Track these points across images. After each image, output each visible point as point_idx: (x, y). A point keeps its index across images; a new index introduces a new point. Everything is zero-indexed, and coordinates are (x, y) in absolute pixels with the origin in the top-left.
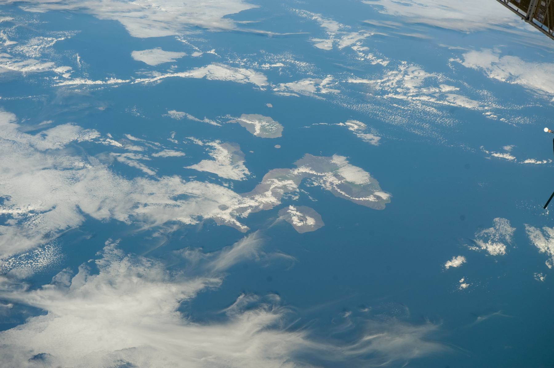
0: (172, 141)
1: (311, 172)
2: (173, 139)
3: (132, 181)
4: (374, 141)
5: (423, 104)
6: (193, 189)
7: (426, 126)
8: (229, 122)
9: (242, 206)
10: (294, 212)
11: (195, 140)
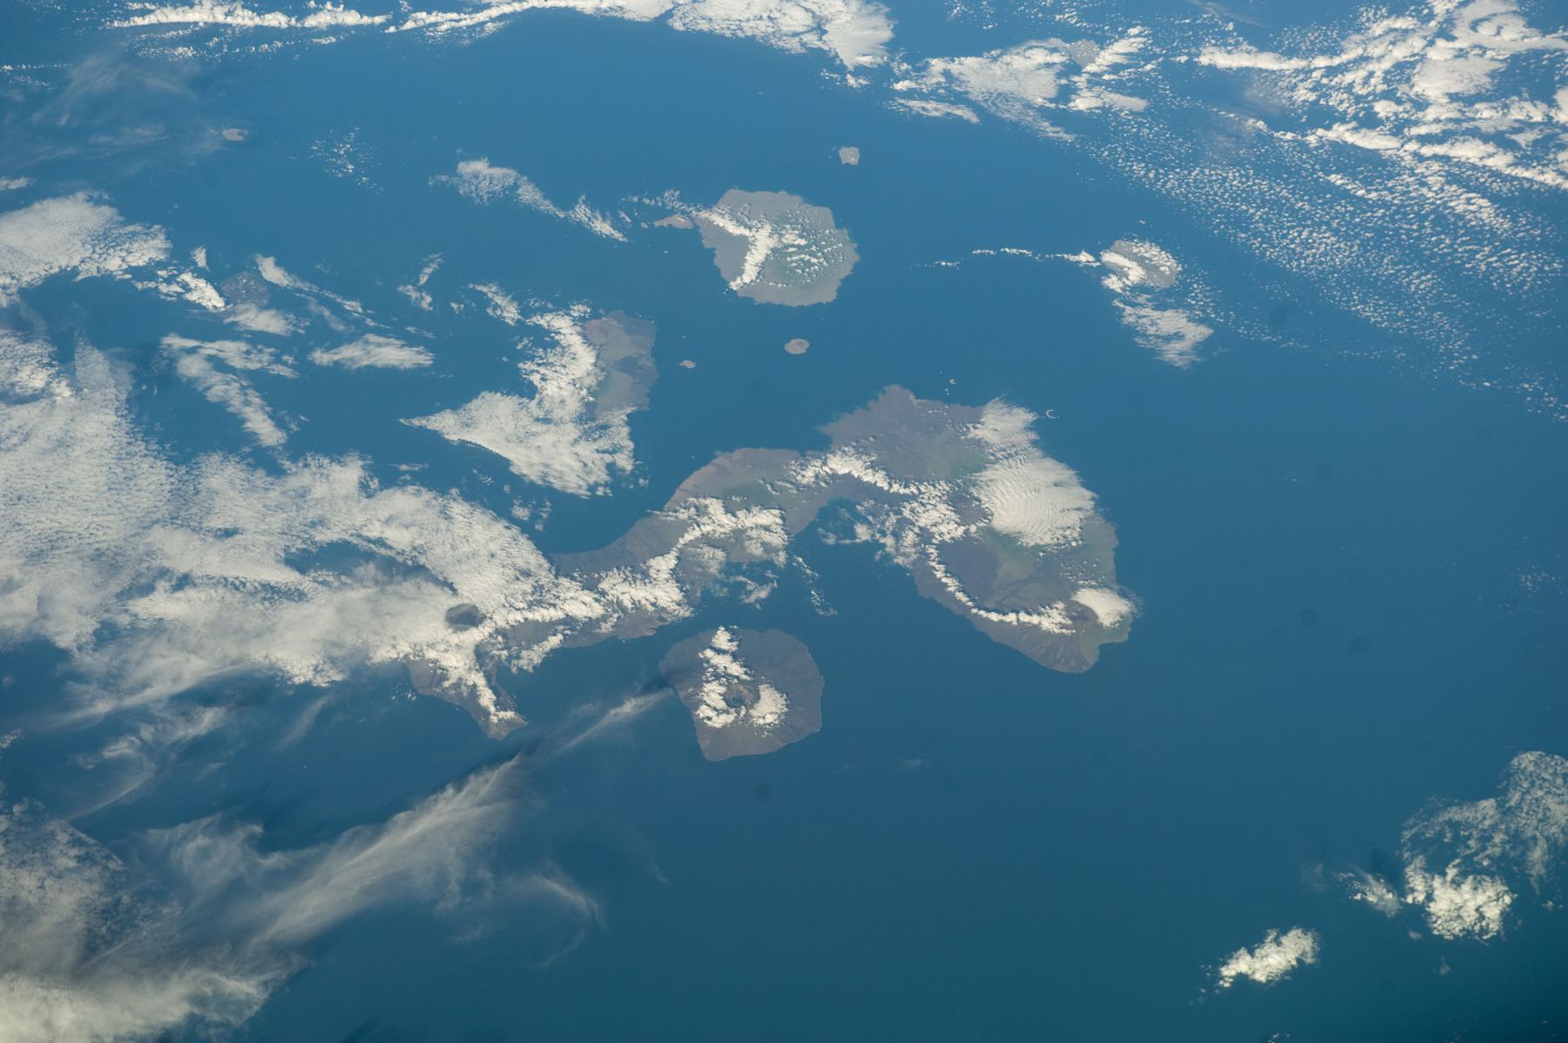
0: (414, 295)
1: (868, 477)
2: (419, 289)
3: (183, 470)
4: (1178, 346)
5: (1452, 179)
6: (388, 521)
7: (1421, 282)
8: (665, 223)
9: (539, 615)
10: (722, 662)
11: (499, 300)
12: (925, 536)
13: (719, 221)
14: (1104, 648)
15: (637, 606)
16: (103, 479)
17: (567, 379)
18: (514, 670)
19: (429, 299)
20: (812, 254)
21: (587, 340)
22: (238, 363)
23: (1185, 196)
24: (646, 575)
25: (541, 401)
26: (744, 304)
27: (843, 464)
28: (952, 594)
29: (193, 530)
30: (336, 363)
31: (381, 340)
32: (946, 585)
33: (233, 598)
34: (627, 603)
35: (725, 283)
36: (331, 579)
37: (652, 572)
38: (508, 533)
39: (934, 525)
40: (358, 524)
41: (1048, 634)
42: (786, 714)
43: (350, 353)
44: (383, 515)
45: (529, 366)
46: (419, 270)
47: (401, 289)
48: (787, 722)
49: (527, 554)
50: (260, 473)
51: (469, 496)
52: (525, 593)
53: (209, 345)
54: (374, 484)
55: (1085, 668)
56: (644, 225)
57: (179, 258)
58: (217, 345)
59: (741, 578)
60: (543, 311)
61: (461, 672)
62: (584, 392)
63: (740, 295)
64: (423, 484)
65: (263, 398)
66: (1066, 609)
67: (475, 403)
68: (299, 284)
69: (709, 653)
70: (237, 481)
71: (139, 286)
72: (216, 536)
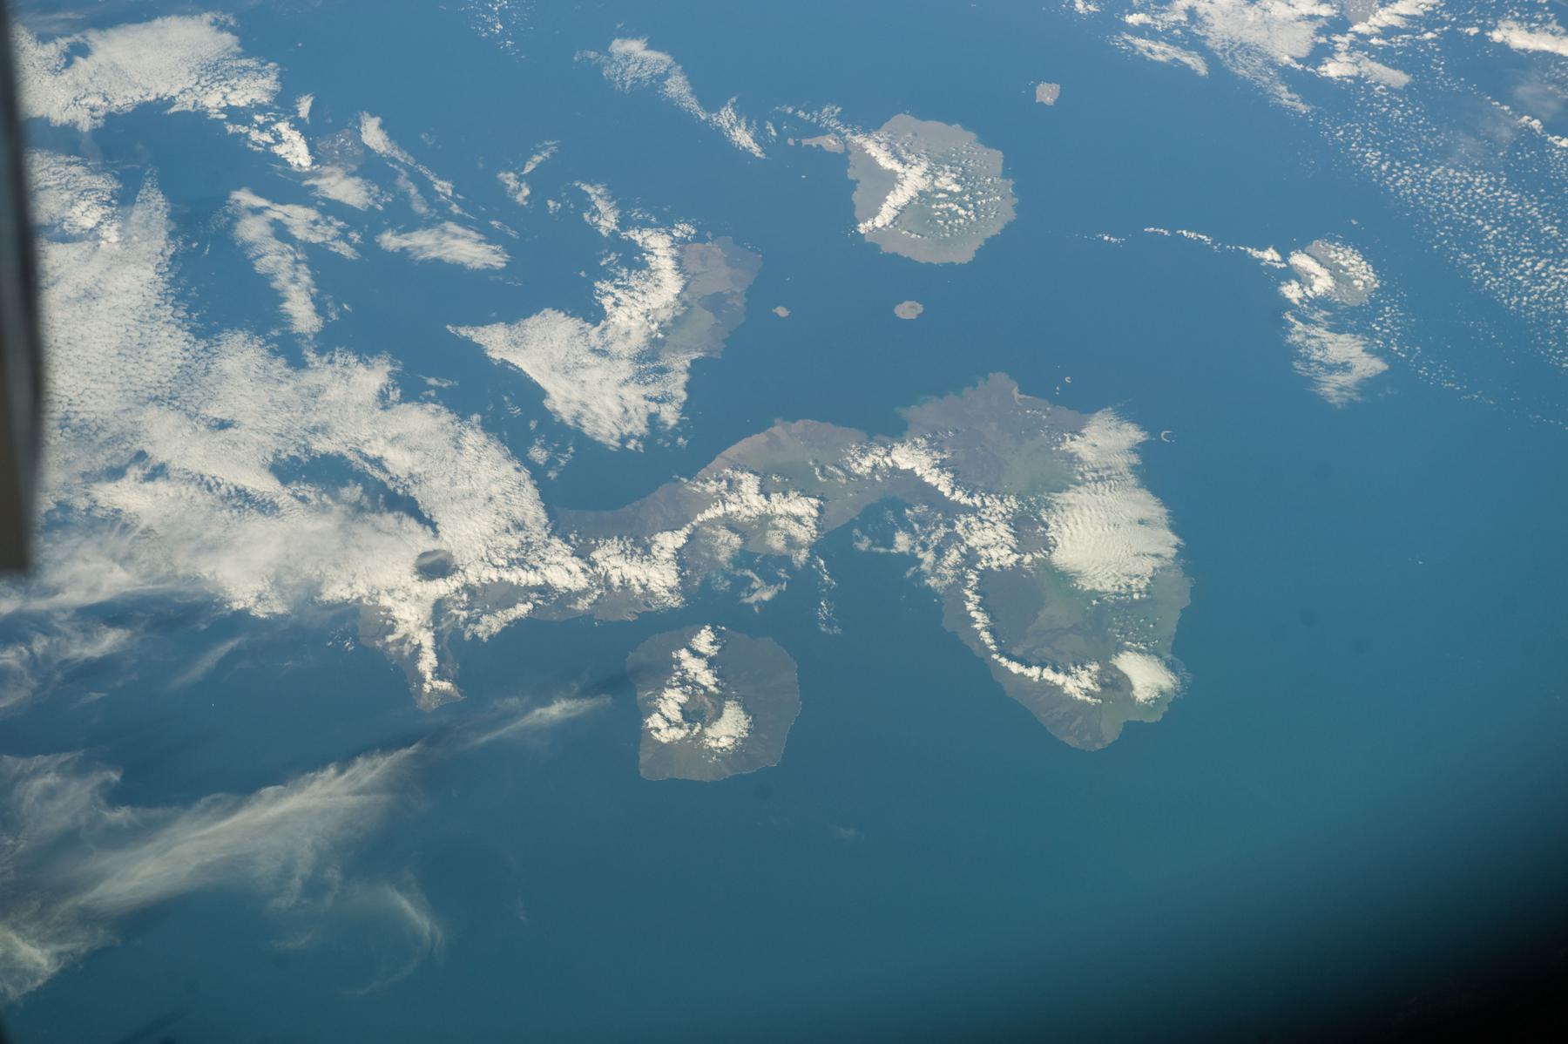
0: (513, 184)
1: (932, 478)
2: (520, 179)
3: (202, 344)
4: (1341, 379)
6: (393, 441)
8: (814, 143)
10: (694, 666)
11: (601, 205)
12: (971, 558)
13: (872, 149)
14: (1128, 725)
15: (625, 585)
16: (116, 341)
17: (641, 308)
18: (468, 635)
19: (526, 192)
20: (963, 205)
22: (300, 233)
23: (1415, 199)
24: (647, 550)
25: (605, 329)
26: (868, 250)
27: (910, 458)
28: (977, 632)
29: (189, 416)
30: (403, 249)
32: (974, 620)
33: (203, 499)
34: (615, 581)
35: (855, 222)
36: (311, 496)
39: (985, 547)
41: (1070, 699)
42: (744, 740)
43: (424, 242)
44: (391, 432)
45: (606, 286)
46: (528, 157)
48: (743, 748)
49: (529, 506)
50: (280, 361)
51: (489, 427)
52: (510, 549)
53: (279, 207)
54: (395, 395)
55: (1099, 746)
56: (791, 142)
57: (282, 105)
58: (286, 209)
59: (749, 573)
60: (644, 225)
61: (412, 627)
62: (654, 327)
63: (868, 240)
64: (446, 405)
65: (313, 277)
66: (1101, 674)
67: (535, 320)
68: (396, 153)
69: (684, 654)
70: (253, 368)
71: (231, 129)
72: (209, 426)
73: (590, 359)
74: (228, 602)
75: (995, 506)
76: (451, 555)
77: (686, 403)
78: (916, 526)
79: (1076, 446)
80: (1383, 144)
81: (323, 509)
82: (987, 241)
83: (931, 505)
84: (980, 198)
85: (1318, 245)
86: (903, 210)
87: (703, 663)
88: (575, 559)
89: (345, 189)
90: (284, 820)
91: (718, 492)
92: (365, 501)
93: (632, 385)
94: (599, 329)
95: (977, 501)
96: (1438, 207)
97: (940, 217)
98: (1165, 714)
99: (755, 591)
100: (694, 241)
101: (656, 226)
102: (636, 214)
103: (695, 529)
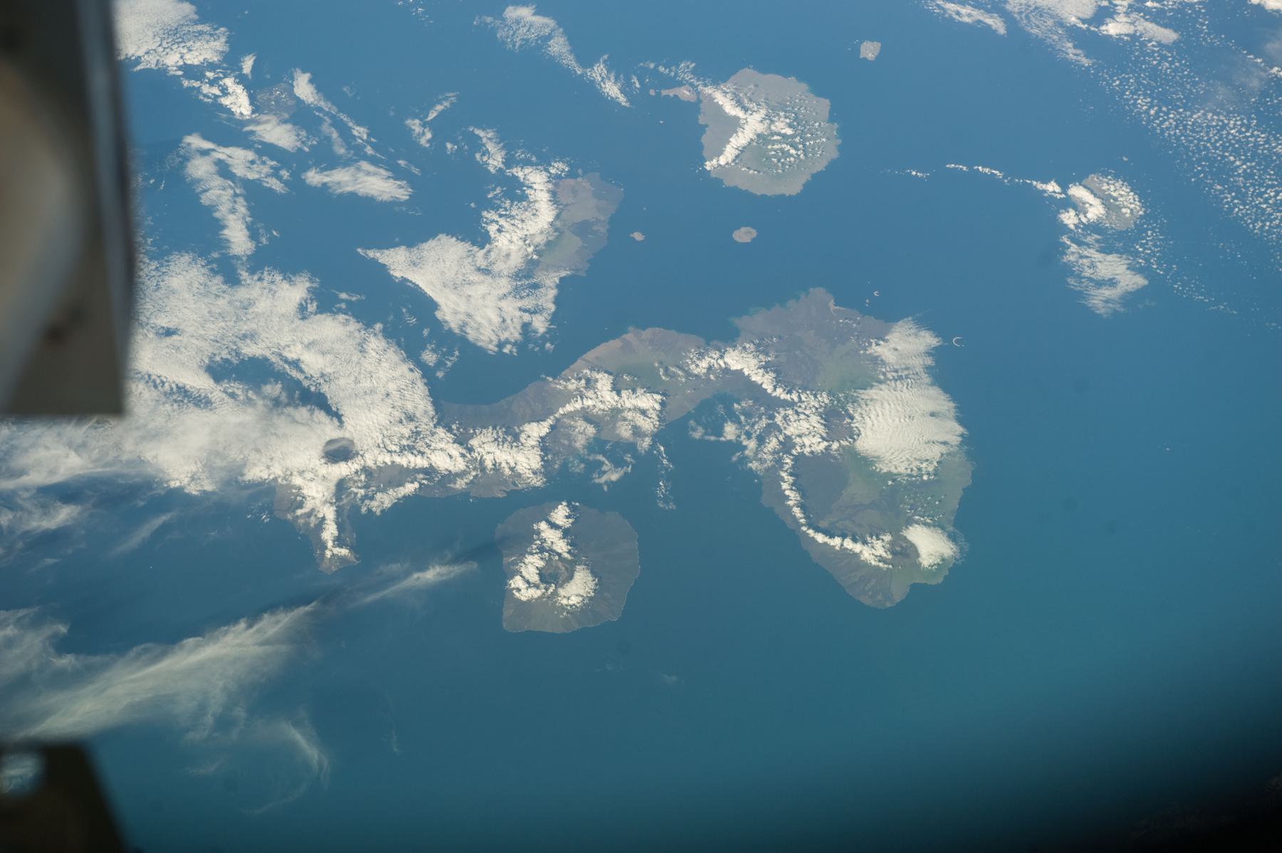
2: (424, 125)
4: (1107, 293)
6: (309, 346)
8: (671, 93)
10: (552, 537)
11: (491, 147)
12: (787, 445)
14: (914, 586)
17: (520, 234)
18: (364, 510)
19: (429, 136)
20: (794, 146)
21: (554, 197)
22: (239, 171)
23: (1178, 139)
24: (516, 438)
25: (489, 251)
26: (713, 184)
27: (740, 361)
28: (790, 508)
30: (324, 184)
31: (371, 168)
32: (787, 498)
34: (489, 464)
35: (703, 160)
36: (239, 392)
37: (523, 437)
38: (409, 375)
39: (800, 436)
40: (283, 344)
41: (866, 564)
42: (591, 599)
43: (342, 179)
45: (491, 215)
46: (431, 106)
47: (409, 122)
48: (590, 605)
49: (419, 401)
50: (218, 279)
51: (388, 334)
52: (402, 437)
53: (222, 149)
54: (312, 307)
55: (888, 605)
56: (652, 92)
58: (229, 151)
59: (601, 458)
60: (526, 163)
62: (530, 249)
63: (713, 175)
64: (354, 316)
65: (249, 208)
66: (892, 543)
67: (431, 243)
68: (322, 104)
69: (543, 526)
70: (196, 284)
72: (157, 334)
73: (475, 277)
74: (167, 482)
75: (810, 401)
76: (352, 442)
77: (554, 314)
78: (742, 418)
79: (881, 350)
80: (1153, 92)
81: (249, 401)
82: (813, 176)
83: (756, 400)
84: (809, 140)
85: (1093, 178)
86: (743, 150)
87: (559, 533)
88: (456, 445)
89: (279, 134)
90: (201, 666)
91: (577, 389)
92: (284, 398)
93: (510, 298)
94: (484, 251)
95: (795, 396)
96: (1197, 146)
97: (774, 156)
98: (946, 577)
99: (605, 472)
100: (567, 176)
101: (537, 164)
102: (519, 154)
103: (558, 420)
